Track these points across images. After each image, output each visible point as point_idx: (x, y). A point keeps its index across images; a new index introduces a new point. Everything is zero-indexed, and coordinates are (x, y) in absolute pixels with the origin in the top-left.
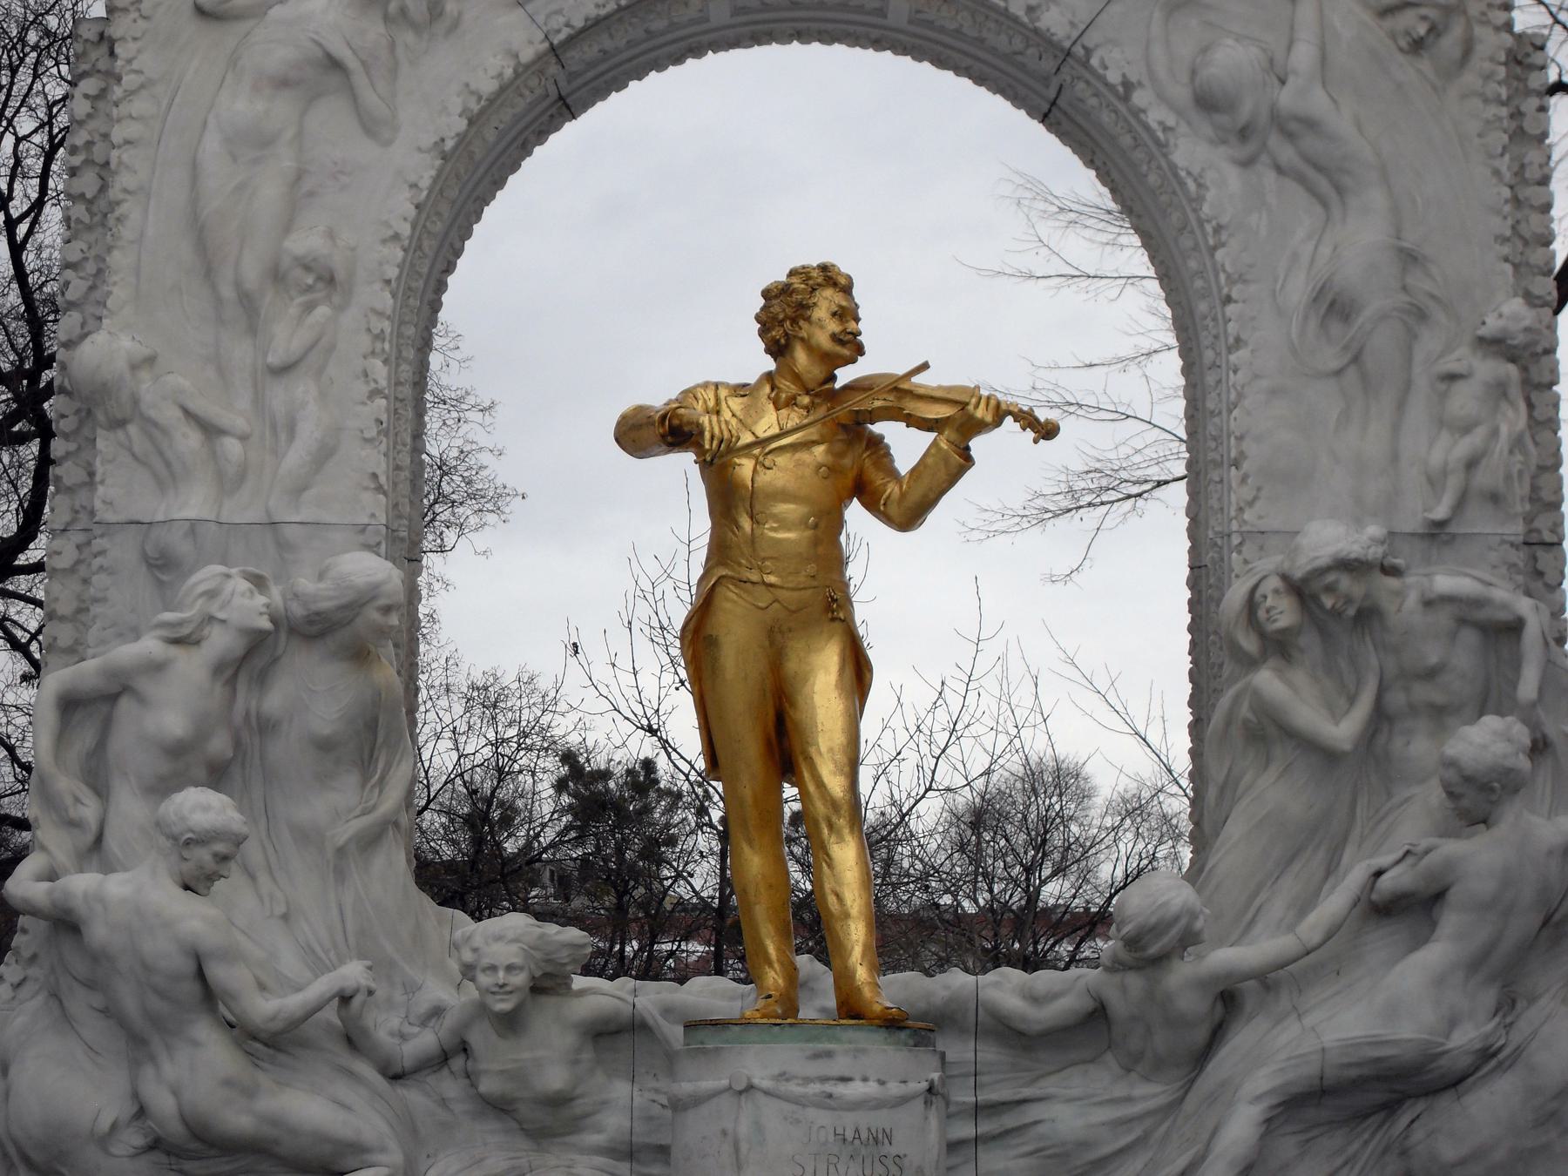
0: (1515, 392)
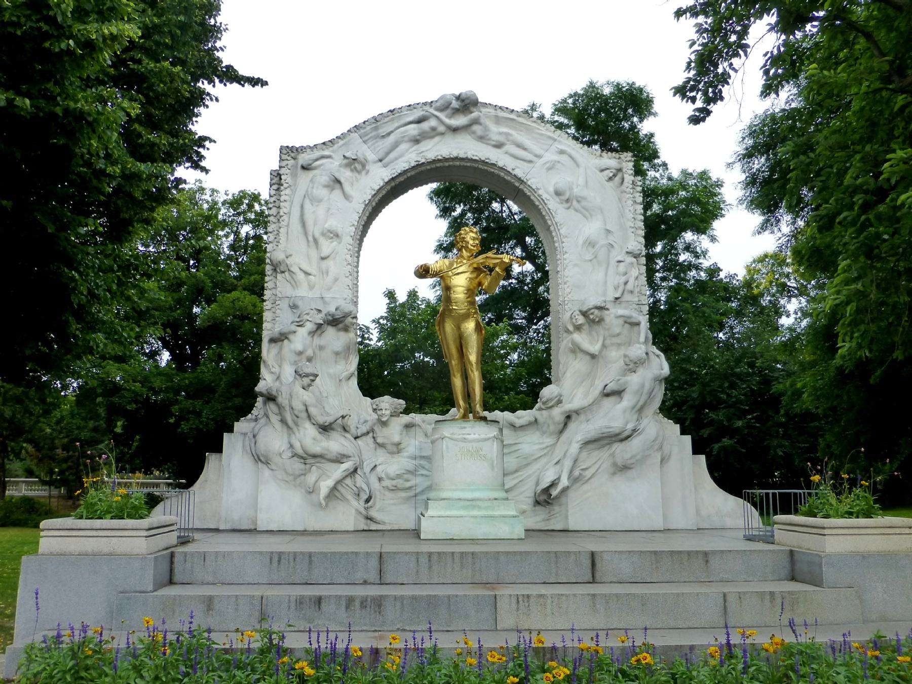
0: (635, 264)
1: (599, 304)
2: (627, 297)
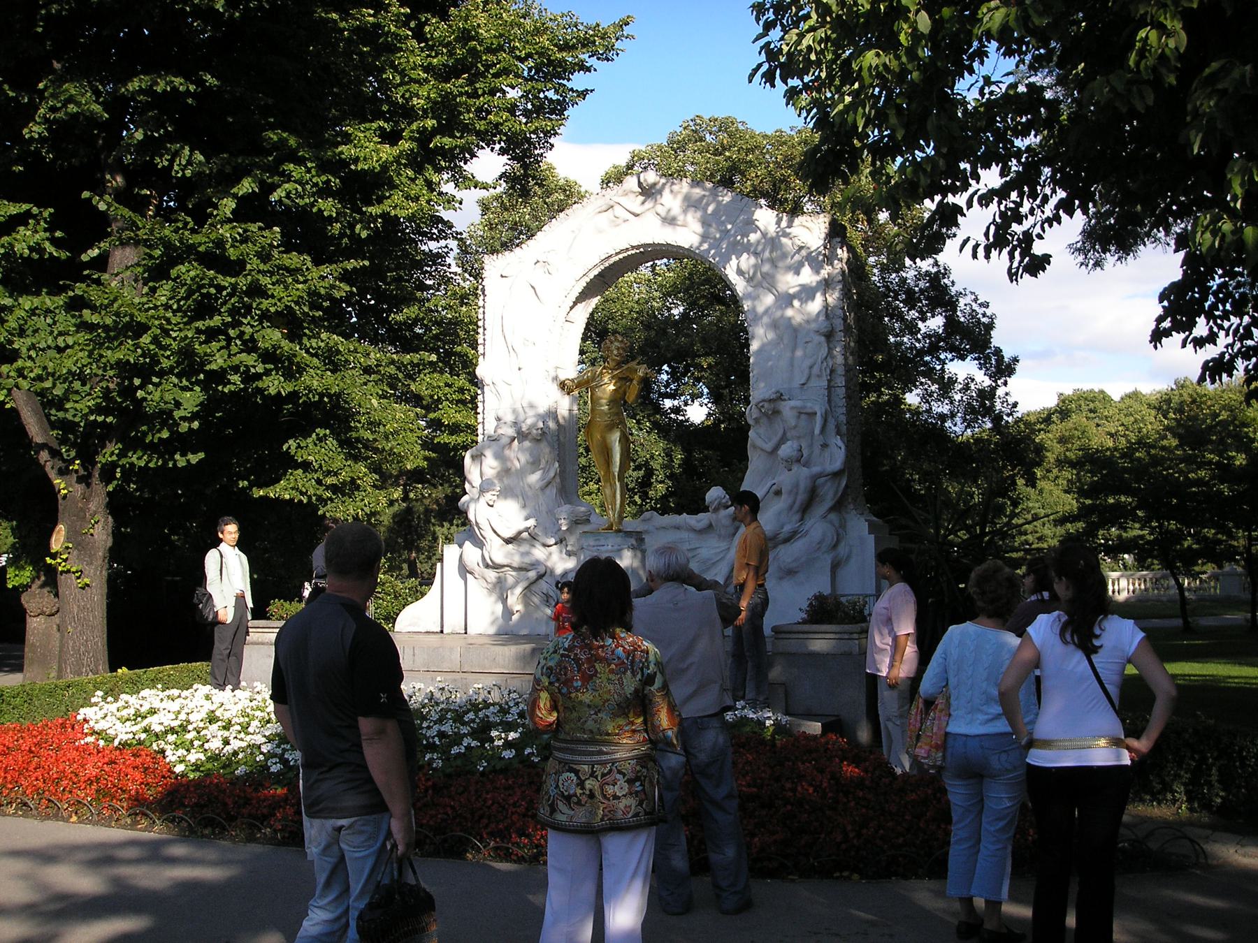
1: (767, 396)
2: (814, 383)
